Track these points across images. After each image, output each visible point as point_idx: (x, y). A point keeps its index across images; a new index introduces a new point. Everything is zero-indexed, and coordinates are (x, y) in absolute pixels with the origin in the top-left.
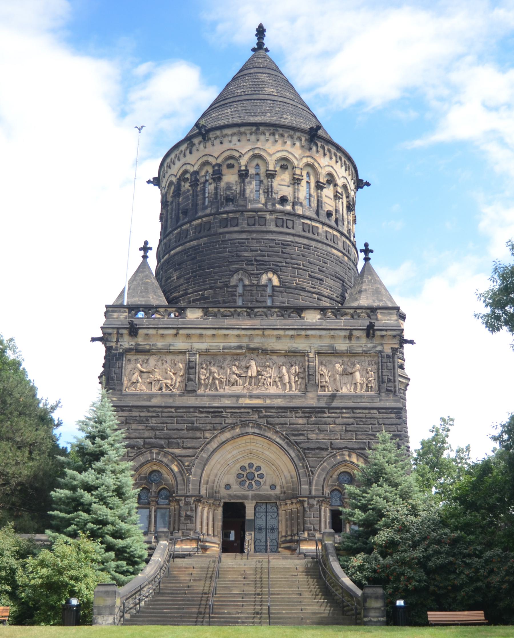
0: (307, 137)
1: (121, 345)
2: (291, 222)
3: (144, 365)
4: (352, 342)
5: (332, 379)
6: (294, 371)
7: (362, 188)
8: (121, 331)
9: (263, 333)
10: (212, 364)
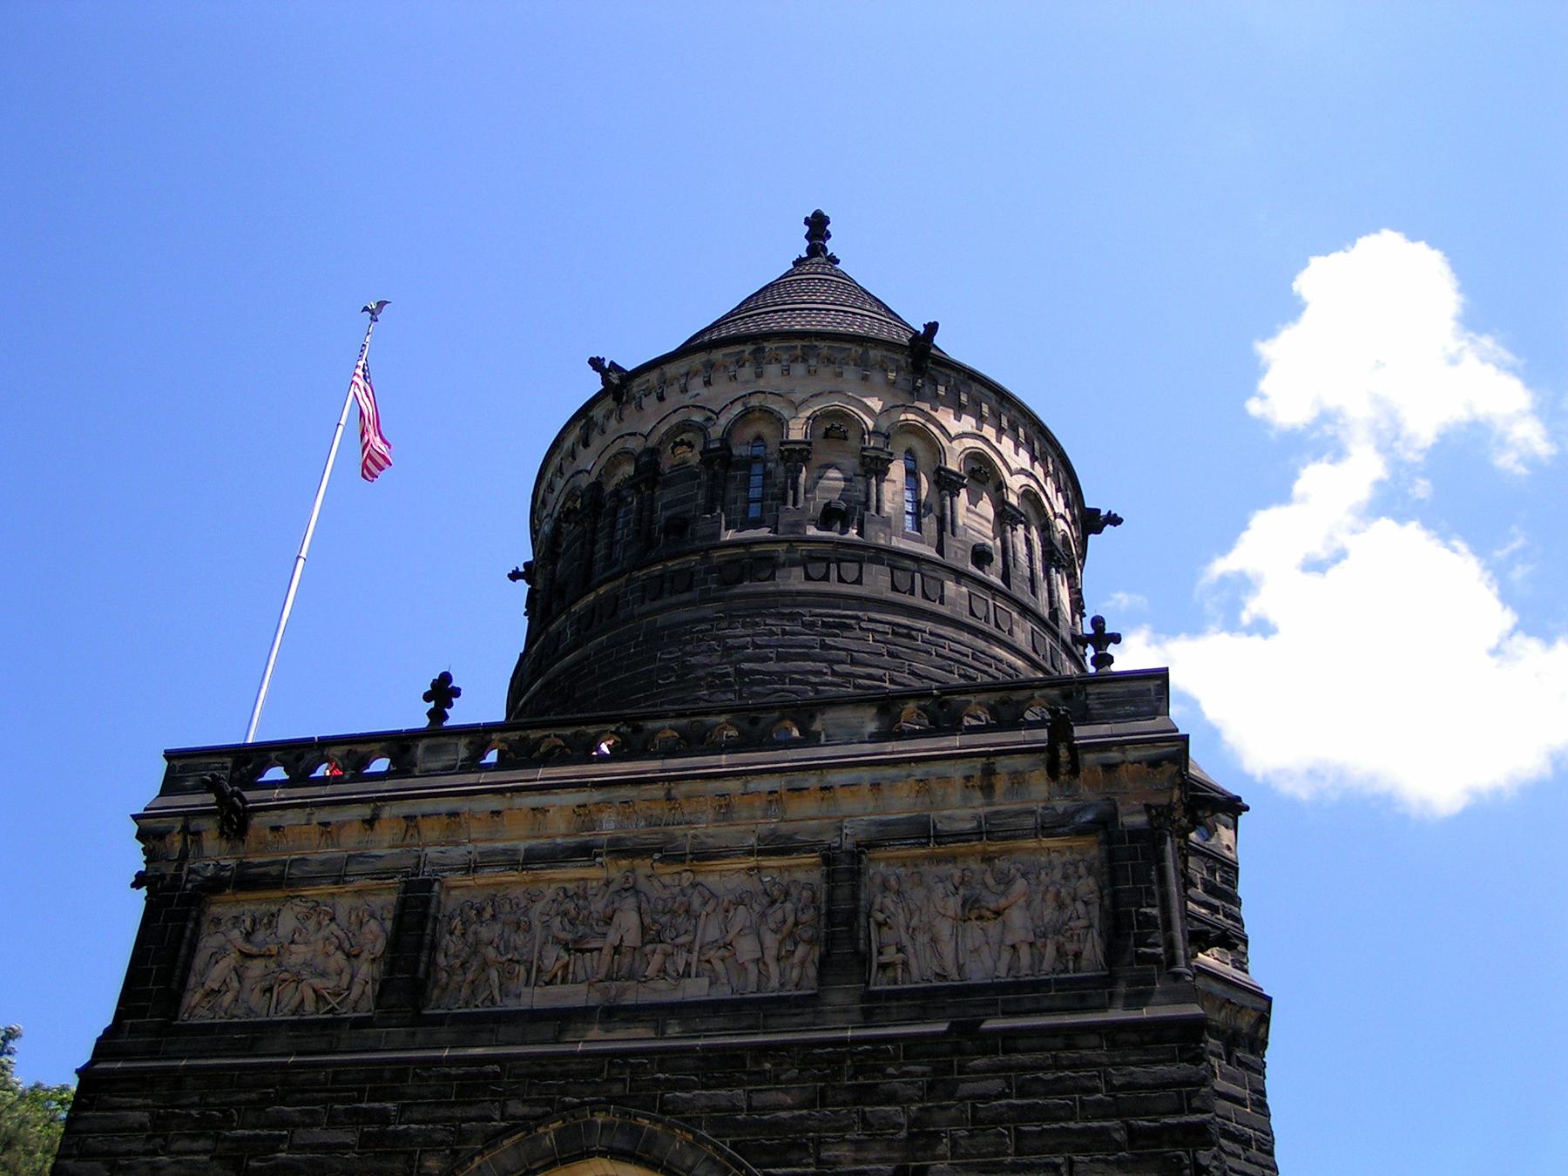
0: (902, 359)
1: (191, 871)
2: (855, 566)
3: (260, 936)
4: (996, 799)
5: (922, 939)
6: (779, 915)
7: (1098, 531)
8: (195, 824)
9: (669, 798)
10: (487, 915)
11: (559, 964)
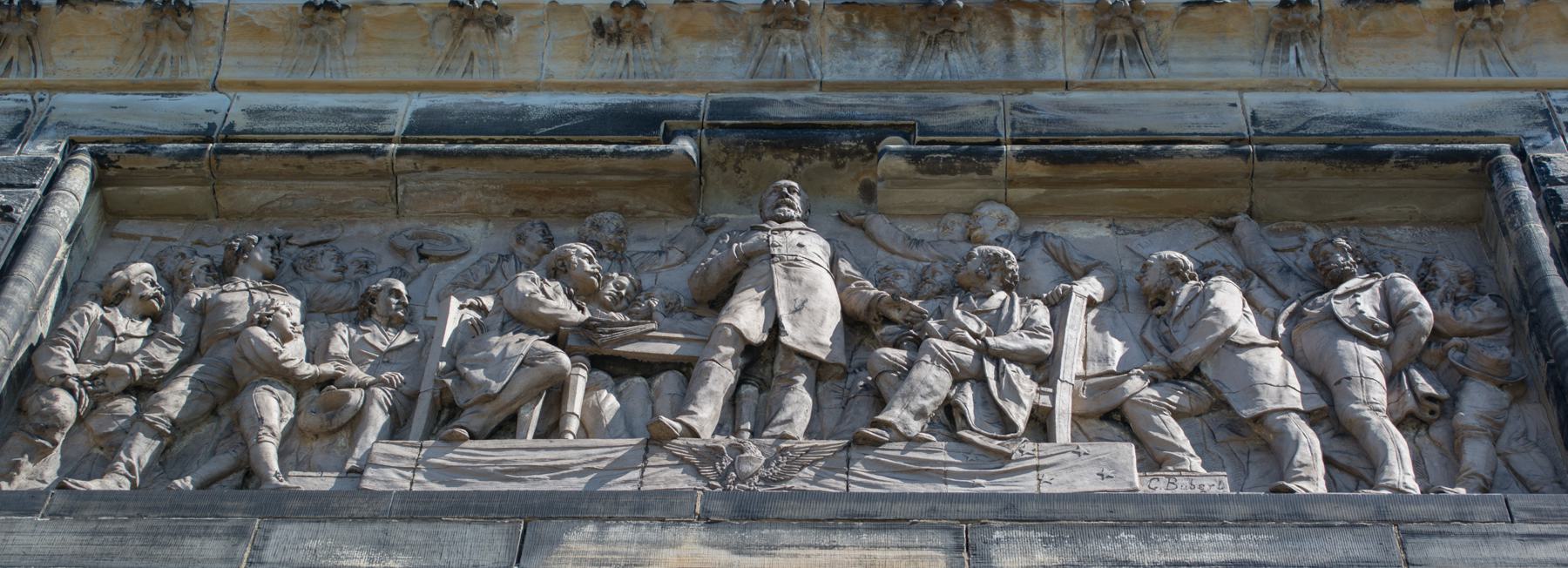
6: (1368, 304)
11: (531, 376)
